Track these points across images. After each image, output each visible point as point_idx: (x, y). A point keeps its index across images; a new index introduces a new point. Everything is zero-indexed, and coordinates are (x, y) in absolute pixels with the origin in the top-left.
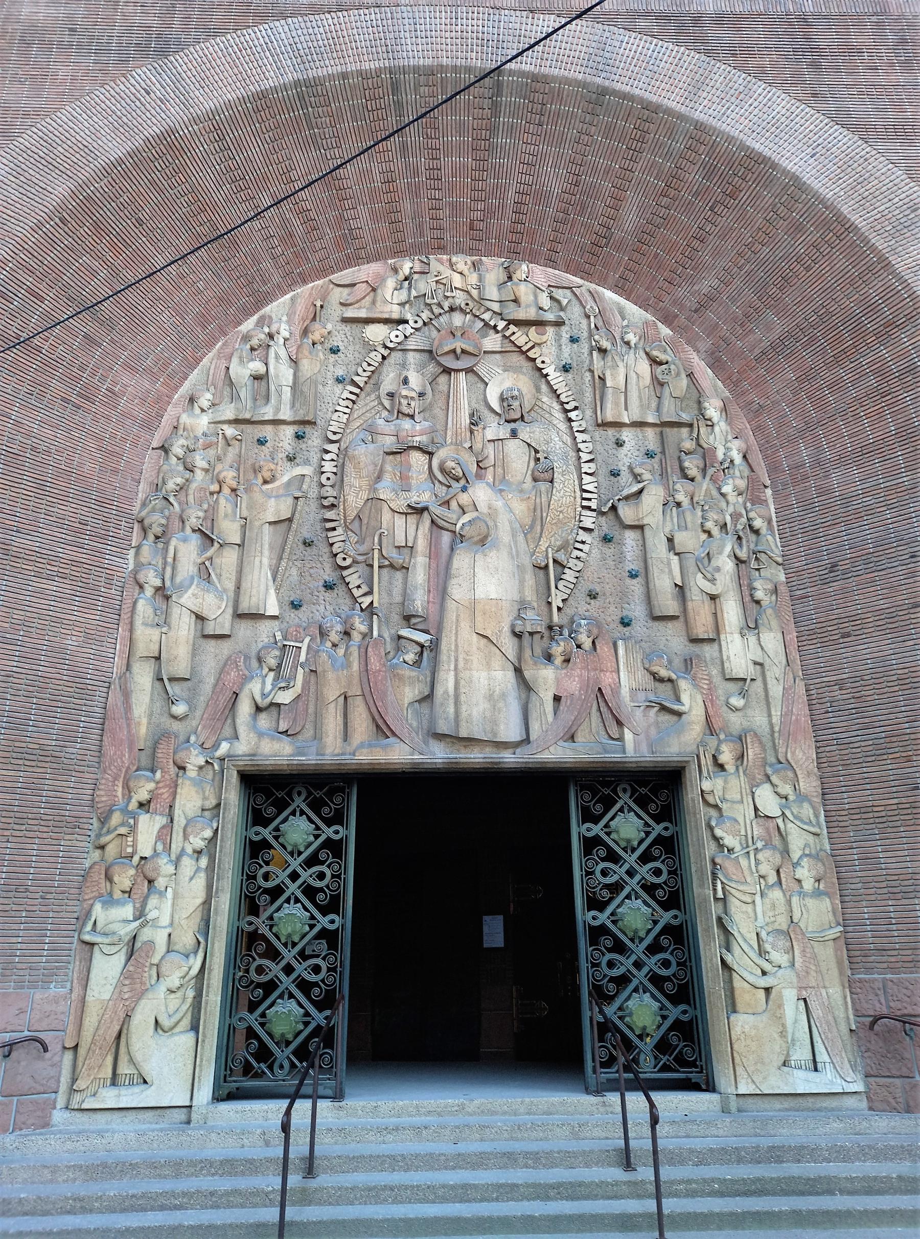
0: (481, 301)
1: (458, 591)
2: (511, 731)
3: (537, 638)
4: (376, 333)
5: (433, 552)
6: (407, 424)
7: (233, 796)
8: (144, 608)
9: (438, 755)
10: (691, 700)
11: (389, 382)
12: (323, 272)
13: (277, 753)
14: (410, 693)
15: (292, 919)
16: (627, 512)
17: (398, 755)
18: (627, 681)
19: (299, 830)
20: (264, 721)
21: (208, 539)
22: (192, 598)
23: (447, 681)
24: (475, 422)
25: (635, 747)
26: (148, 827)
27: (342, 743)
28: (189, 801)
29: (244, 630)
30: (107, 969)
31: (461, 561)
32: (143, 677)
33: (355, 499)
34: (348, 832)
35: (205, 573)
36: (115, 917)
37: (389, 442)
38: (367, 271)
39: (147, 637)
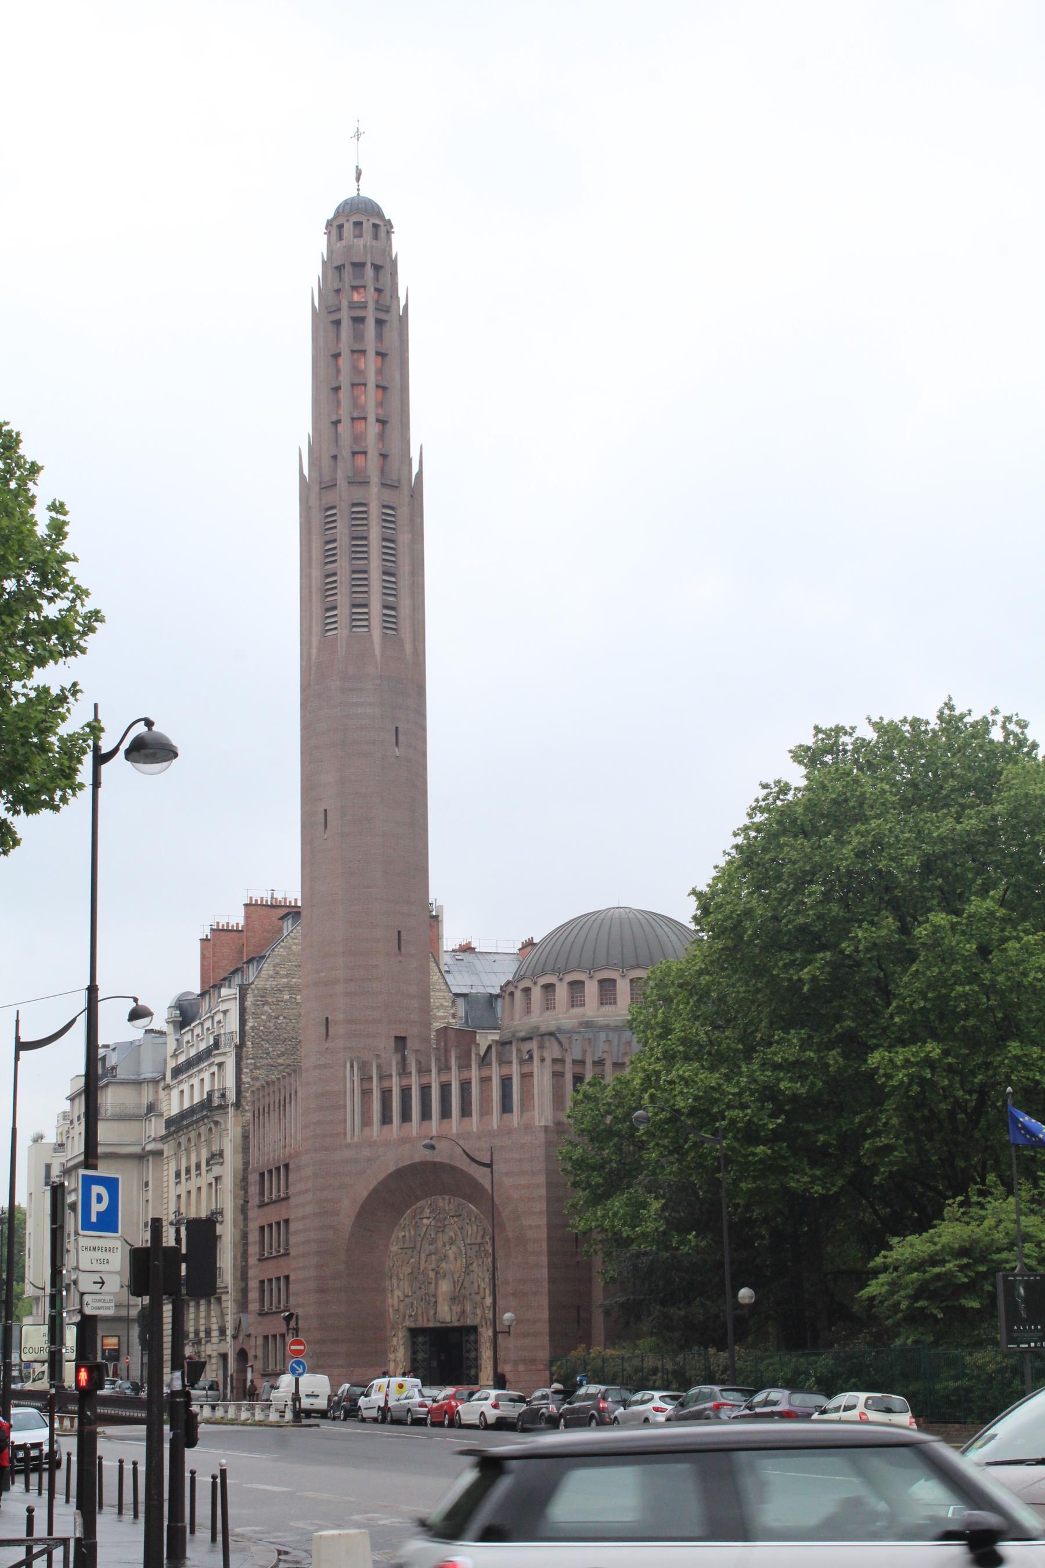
0: (445, 1210)
1: (440, 1290)
2: (448, 1320)
3: (453, 1299)
4: (425, 1221)
5: (436, 1280)
6: (431, 1247)
7: (408, 1334)
8: (389, 1295)
9: (438, 1325)
10: (479, 1312)
11: (428, 1236)
12: (413, 1204)
13: (412, 1325)
14: (432, 1312)
15: (420, 1356)
16: (471, 1268)
17: (431, 1325)
18: (468, 1308)
19: (420, 1339)
20: (412, 1319)
21: (399, 1279)
22: (397, 1293)
23: (439, 1309)
24: (444, 1245)
25: (469, 1322)
26: (395, 1340)
27: (421, 1323)
28: (400, 1335)
29: (407, 1299)
30: (392, 1365)
31: (440, 1282)
32: (391, 1310)
33: (422, 1268)
34: (427, 1339)
35: (398, 1286)
36: (392, 1356)
37: (427, 1252)
38: (422, 1203)
39: (390, 1301)
